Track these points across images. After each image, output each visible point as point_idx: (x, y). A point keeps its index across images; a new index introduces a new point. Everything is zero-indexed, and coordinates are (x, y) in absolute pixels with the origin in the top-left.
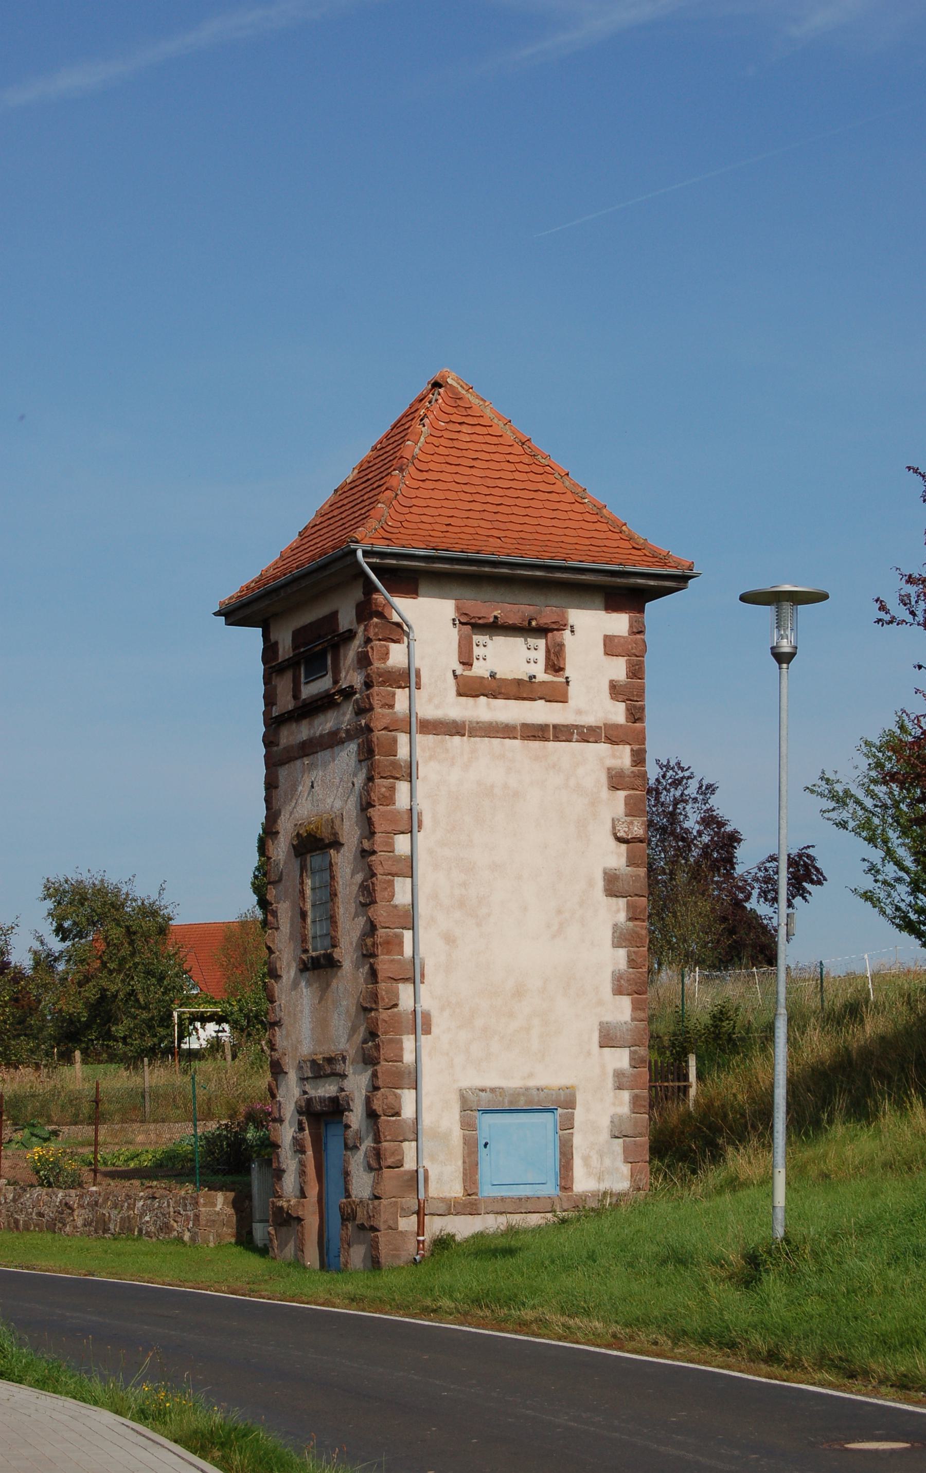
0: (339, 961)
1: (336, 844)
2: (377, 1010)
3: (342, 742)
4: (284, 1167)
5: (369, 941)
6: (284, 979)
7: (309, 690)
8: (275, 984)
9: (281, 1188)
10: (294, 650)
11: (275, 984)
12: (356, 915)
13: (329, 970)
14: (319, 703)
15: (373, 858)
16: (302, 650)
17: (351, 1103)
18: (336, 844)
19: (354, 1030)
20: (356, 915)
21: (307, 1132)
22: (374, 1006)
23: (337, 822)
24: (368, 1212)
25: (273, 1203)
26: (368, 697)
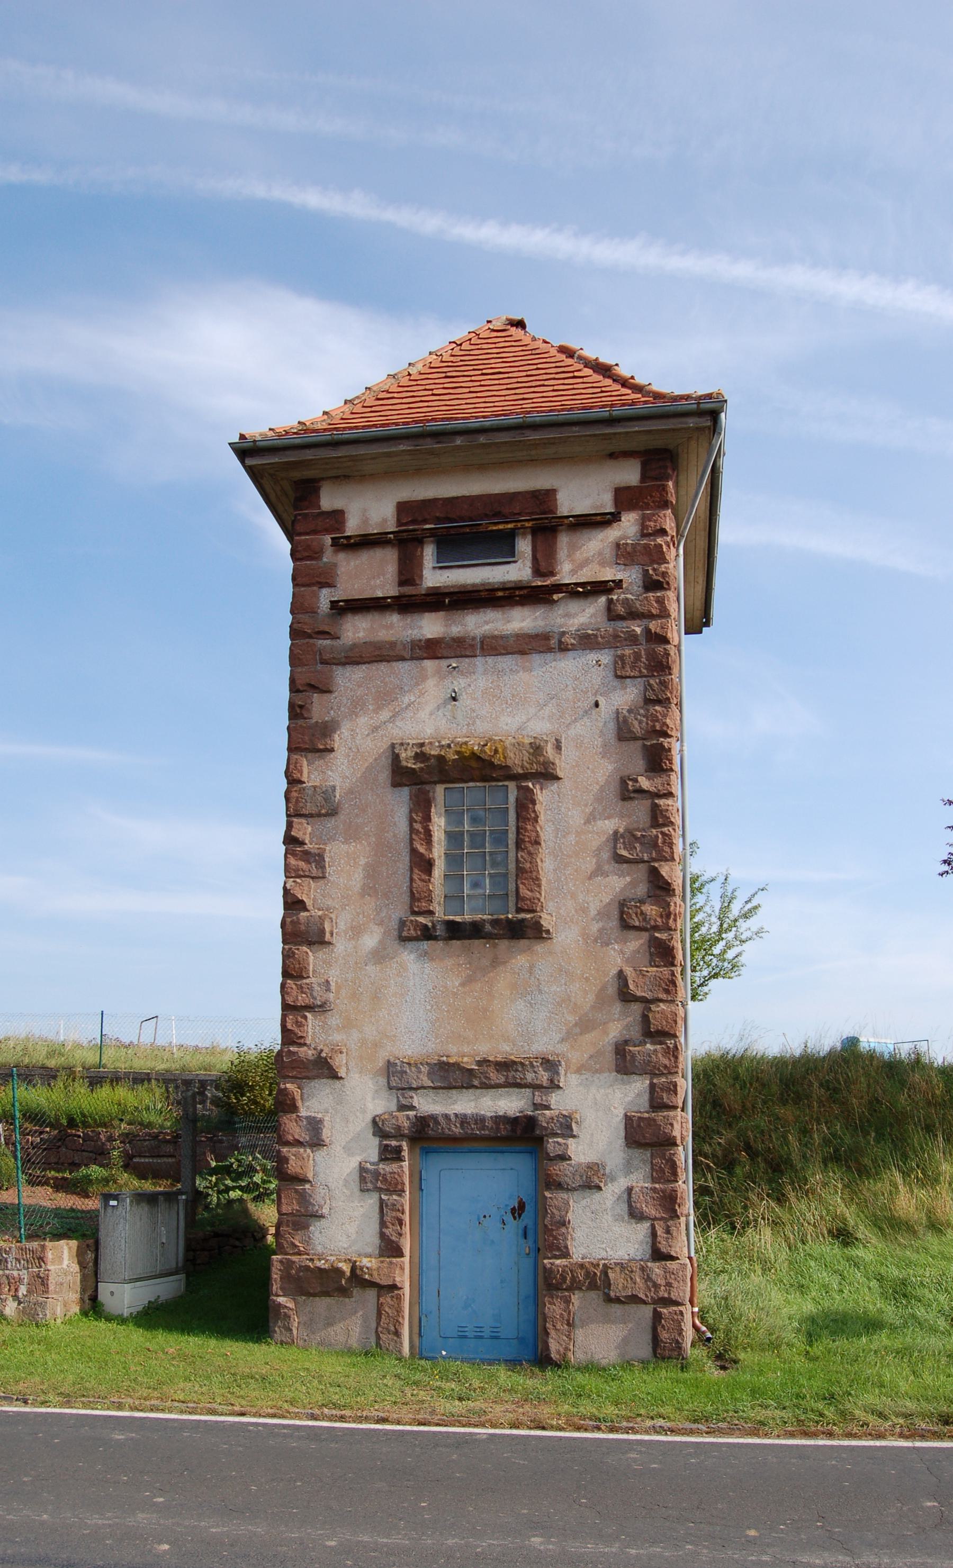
0: (548, 932)
1: (548, 775)
2: (673, 1001)
3: (563, 648)
4: (325, 1211)
5: (651, 910)
6: (341, 946)
7: (434, 576)
8: (310, 954)
9: (308, 1241)
10: (399, 523)
11: (310, 954)
12: (599, 871)
13: (504, 944)
14: (500, 594)
15: (670, 802)
16: (428, 526)
17: (574, 1125)
18: (548, 775)
19: (585, 1025)
20: (599, 871)
21: (407, 1163)
22: (663, 996)
23: (550, 751)
24: (648, 1279)
25: (288, 1264)
26: (661, 601)
